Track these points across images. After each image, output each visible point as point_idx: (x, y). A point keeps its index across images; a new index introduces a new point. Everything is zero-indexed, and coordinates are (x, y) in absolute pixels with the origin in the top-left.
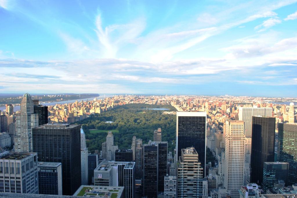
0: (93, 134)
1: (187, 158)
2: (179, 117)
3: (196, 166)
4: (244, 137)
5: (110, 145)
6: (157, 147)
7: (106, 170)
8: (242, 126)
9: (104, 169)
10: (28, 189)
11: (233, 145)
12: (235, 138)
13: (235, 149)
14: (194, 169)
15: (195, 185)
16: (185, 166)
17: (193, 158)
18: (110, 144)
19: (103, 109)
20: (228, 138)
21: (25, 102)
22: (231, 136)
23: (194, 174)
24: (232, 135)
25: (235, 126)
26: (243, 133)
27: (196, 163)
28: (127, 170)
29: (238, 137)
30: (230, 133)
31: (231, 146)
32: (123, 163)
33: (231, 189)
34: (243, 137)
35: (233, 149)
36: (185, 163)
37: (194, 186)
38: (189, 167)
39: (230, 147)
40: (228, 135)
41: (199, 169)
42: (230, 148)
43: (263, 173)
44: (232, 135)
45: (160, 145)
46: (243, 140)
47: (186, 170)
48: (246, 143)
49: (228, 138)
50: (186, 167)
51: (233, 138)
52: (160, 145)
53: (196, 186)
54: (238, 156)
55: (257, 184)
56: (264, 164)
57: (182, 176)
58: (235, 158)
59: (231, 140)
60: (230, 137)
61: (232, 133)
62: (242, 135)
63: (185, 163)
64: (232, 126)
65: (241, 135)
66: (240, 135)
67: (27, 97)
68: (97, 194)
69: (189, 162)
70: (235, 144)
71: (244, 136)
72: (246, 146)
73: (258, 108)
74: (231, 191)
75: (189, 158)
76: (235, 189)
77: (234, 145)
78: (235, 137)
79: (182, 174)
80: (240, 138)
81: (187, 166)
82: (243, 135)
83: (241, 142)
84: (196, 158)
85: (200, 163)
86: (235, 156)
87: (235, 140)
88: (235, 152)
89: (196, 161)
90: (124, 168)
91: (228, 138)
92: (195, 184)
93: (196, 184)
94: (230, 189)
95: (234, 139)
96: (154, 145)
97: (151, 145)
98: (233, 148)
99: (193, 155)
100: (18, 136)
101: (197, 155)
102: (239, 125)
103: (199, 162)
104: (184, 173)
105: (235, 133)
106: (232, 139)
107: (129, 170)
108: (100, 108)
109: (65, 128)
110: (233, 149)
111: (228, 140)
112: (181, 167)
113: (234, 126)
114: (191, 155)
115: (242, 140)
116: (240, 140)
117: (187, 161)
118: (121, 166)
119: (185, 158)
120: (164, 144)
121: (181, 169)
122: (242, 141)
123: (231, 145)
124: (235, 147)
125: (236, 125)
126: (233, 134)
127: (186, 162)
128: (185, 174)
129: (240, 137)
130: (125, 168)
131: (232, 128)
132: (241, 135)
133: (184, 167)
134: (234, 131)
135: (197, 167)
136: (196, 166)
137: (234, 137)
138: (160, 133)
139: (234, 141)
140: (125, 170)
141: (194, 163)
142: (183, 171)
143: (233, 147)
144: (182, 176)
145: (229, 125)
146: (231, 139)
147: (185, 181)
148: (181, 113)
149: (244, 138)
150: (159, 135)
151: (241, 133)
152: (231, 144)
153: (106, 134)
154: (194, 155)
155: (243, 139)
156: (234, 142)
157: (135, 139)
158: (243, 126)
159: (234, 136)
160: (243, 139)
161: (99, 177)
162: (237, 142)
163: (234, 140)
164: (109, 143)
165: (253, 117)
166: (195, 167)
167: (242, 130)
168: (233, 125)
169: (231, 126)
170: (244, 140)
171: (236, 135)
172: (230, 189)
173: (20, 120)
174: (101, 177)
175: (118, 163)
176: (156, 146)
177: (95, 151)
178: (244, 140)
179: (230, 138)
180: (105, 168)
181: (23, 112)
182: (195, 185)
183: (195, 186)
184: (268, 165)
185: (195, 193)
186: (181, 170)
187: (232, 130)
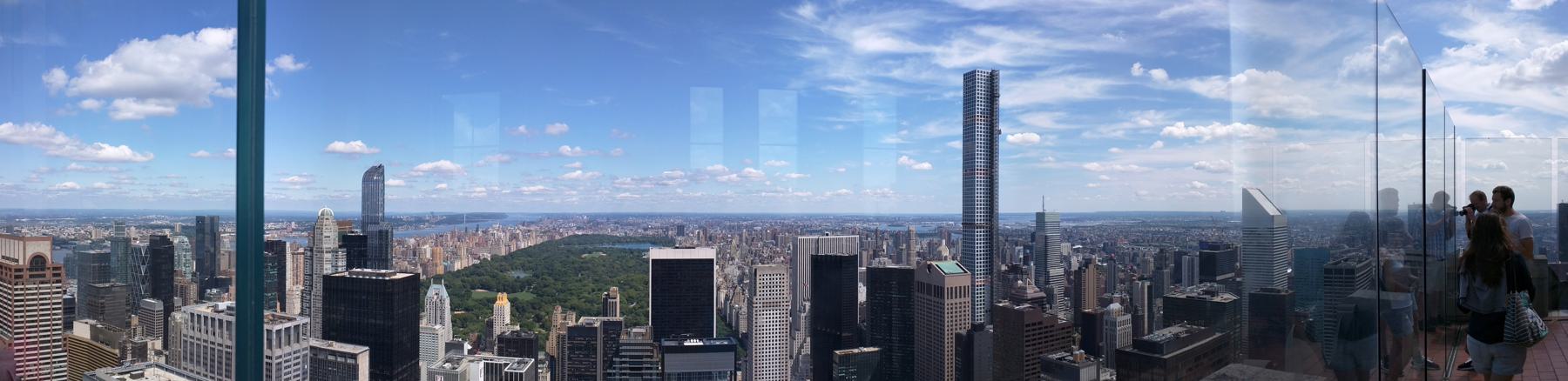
0: (476, 301)
1: (628, 348)
2: (652, 260)
3: (649, 366)
13: (768, 328)
17: (641, 348)
27: (649, 360)
29: (775, 300)
36: (623, 359)
38: (631, 369)
39: (758, 325)
45: (604, 323)
46: (785, 308)
47: (625, 374)
52: (604, 323)
58: (768, 347)
63: (623, 359)
69: (631, 357)
70: (768, 316)
75: (631, 348)
78: (768, 301)
83: (782, 312)
84: (649, 348)
86: (768, 343)
87: (769, 308)
88: (768, 335)
89: (649, 354)
96: (591, 324)
106: (761, 305)
110: (765, 328)
112: (614, 368)
113: (765, 277)
116: (778, 308)
117: (628, 354)
119: (623, 348)
127: (625, 356)
129: (778, 300)
133: (621, 369)
135: (651, 369)
137: (765, 301)
138: (615, 298)
141: (644, 360)
143: (765, 324)
145: (756, 275)
146: (758, 305)
148: (656, 253)
153: (494, 300)
158: (785, 277)
163: (765, 308)
184: (841, 357)
186: (615, 374)
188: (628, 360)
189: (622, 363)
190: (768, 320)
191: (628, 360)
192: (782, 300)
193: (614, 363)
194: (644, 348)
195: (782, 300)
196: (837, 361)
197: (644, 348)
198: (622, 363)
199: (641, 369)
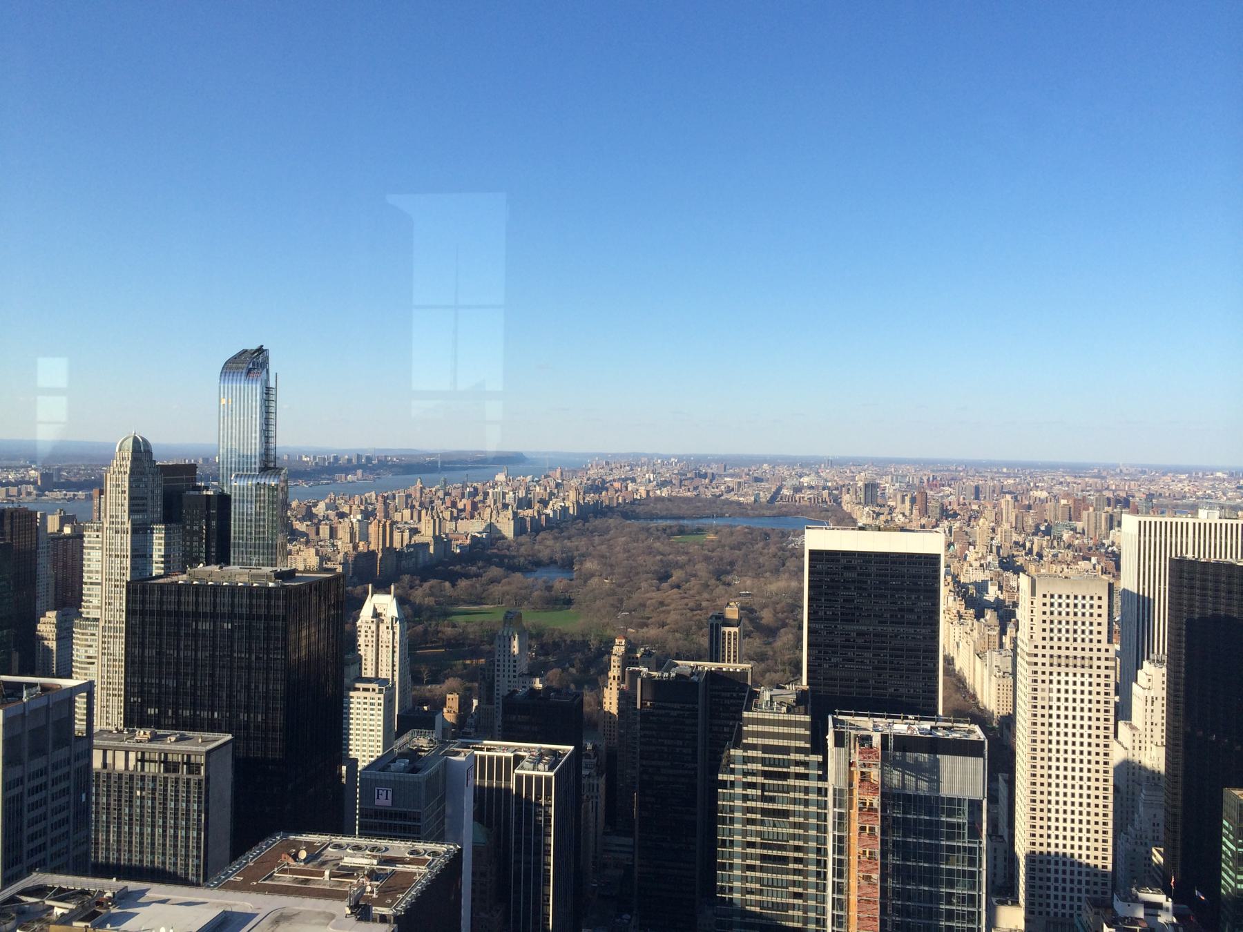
1: (760, 728)
2: (812, 552)
3: (801, 770)
4: (1107, 655)
5: (512, 674)
6: (696, 684)
7: (415, 770)
8: (1096, 602)
9: (405, 767)
10: (32, 838)
11: (1051, 690)
12: (1063, 661)
14: (791, 782)
15: (798, 860)
16: (750, 766)
17: (786, 730)
18: (512, 668)
19: (528, 519)
20: (1027, 658)
21: (125, 473)
22: (1044, 647)
23: (791, 807)
24: (1044, 643)
25: (1064, 601)
26: (1104, 637)
27: (801, 757)
28: (529, 778)
30: (1038, 635)
31: (1043, 699)
32: (520, 749)
33: (1048, 913)
34: (1103, 655)
35: (1054, 712)
36: (750, 753)
37: (791, 866)
38: (766, 775)
39: (1039, 703)
40: (1027, 642)
41: (813, 784)
42: (1035, 707)
43: (1221, 843)
44: (1044, 643)
46: (1103, 672)
47: (753, 786)
48: (1152, 693)
49: (1029, 655)
50: (753, 774)
51: (1052, 656)
53: (801, 867)
54: (1078, 748)
55: (1167, 892)
56: (1225, 798)
57: (738, 815)
59: (1039, 668)
60: (1036, 651)
61: (1047, 634)
62: (1099, 646)
63: (750, 753)
64: (1048, 600)
65: (1095, 645)
66: (1087, 645)
67: (134, 451)
68: (327, 873)
69: (766, 749)
70: (1063, 687)
71: (1107, 650)
72: (1149, 707)
73: (1224, 522)
74: (1048, 923)
75: (767, 729)
76: (1067, 911)
77: (1059, 691)
78: (1063, 653)
79: (738, 803)
80: (1091, 658)
81: (759, 767)
82: (1104, 645)
84: (802, 731)
85: (820, 758)
86: (1062, 747)
89: (802, 744)
90: (516, 771)
91: (1029, 655)
92: (796, 855)
93: (801, 855)
94: (1044, 909)
95: (1055, 661)
97: (673, 675)
98: (1051, 707)
99: (786, 717)
100: (88, 619)
101: (807, 718)
102: (1084, 598)
103: (814, 751)
104: (745, 798)
105: (1064, 635)
106: (1047, 660)
107: (539, 779)
108: (515, 514)
109: (271, 584)
110: (1054, 712)
111: (1026, 666)
112: (732, 771)
113: (1056, 601)
114: (776, 717)
115: (1099, 672)
116: (1087, 671)
117: (760, 741)
118: (508, 759)
119: (750, 728)
120: (735, 672)
121: (732, 778)
122: (1099, 676)
123: (1043, 690)
124: (1062, 704)
125: (1068, 597)
126: (1051, 639)
127: (754, 747)
128: (749, 804)
129: (1087, 654)
130: (522, 768)
131: (1045, 609)
132: (1095, 645)
133: (746, 774)
134: (1055, 626)
135: (805, 777)
136: (801, 770)
137: (1056, 652)
139: (1059, 674)
140: (519, 778)
141: (793, 756)
142: (738, 791)
143: (1055, 704)
144: (738, 815)
147: (749, 839)
148: (818, 539)
149: (1107, 659)
150: (730, 634)
151: (1095, 637)
152: (1040, 685)
154: (792, 717)
155: (1103, 663)
156: (1055, 678)
157: (623, 649)
158: (1105, 603)
159: (1060, 648)
160: (1107, 668)
161: (377, 802)
162: (1071, 679)
163: (1055, 669)
164: (507, 664)
165: (1171, 559)
166: (799, 776)
167: (1099, 620)
168: (1052, 596)
169: (1039, 600)
170: (1107, 672)
171: (1068, 644)
172: (1044, 909)
173: (102, 548)
174: (389, 803)
175: (500, 746)
176: (695, 678)
177: (449, 696)
178: (1107, 672)
179: (1036, 655)
180: (410, 763)
181: (111, 517)
182: (798, 860)
183: (796, 866)
185: (796, 901)
186: (732, 783)
187: (1045, 617)
188: (759, 754)
189: (746, 760)
190: (1063, 695)
191: (759, 754)
192: (1095, 654)
193: (731, 760)
194: (792, 730)
195: (1095, 654)
196: (1235, 814)
197: (792, 730)
198: (746, 760)
199: (785, 776)
